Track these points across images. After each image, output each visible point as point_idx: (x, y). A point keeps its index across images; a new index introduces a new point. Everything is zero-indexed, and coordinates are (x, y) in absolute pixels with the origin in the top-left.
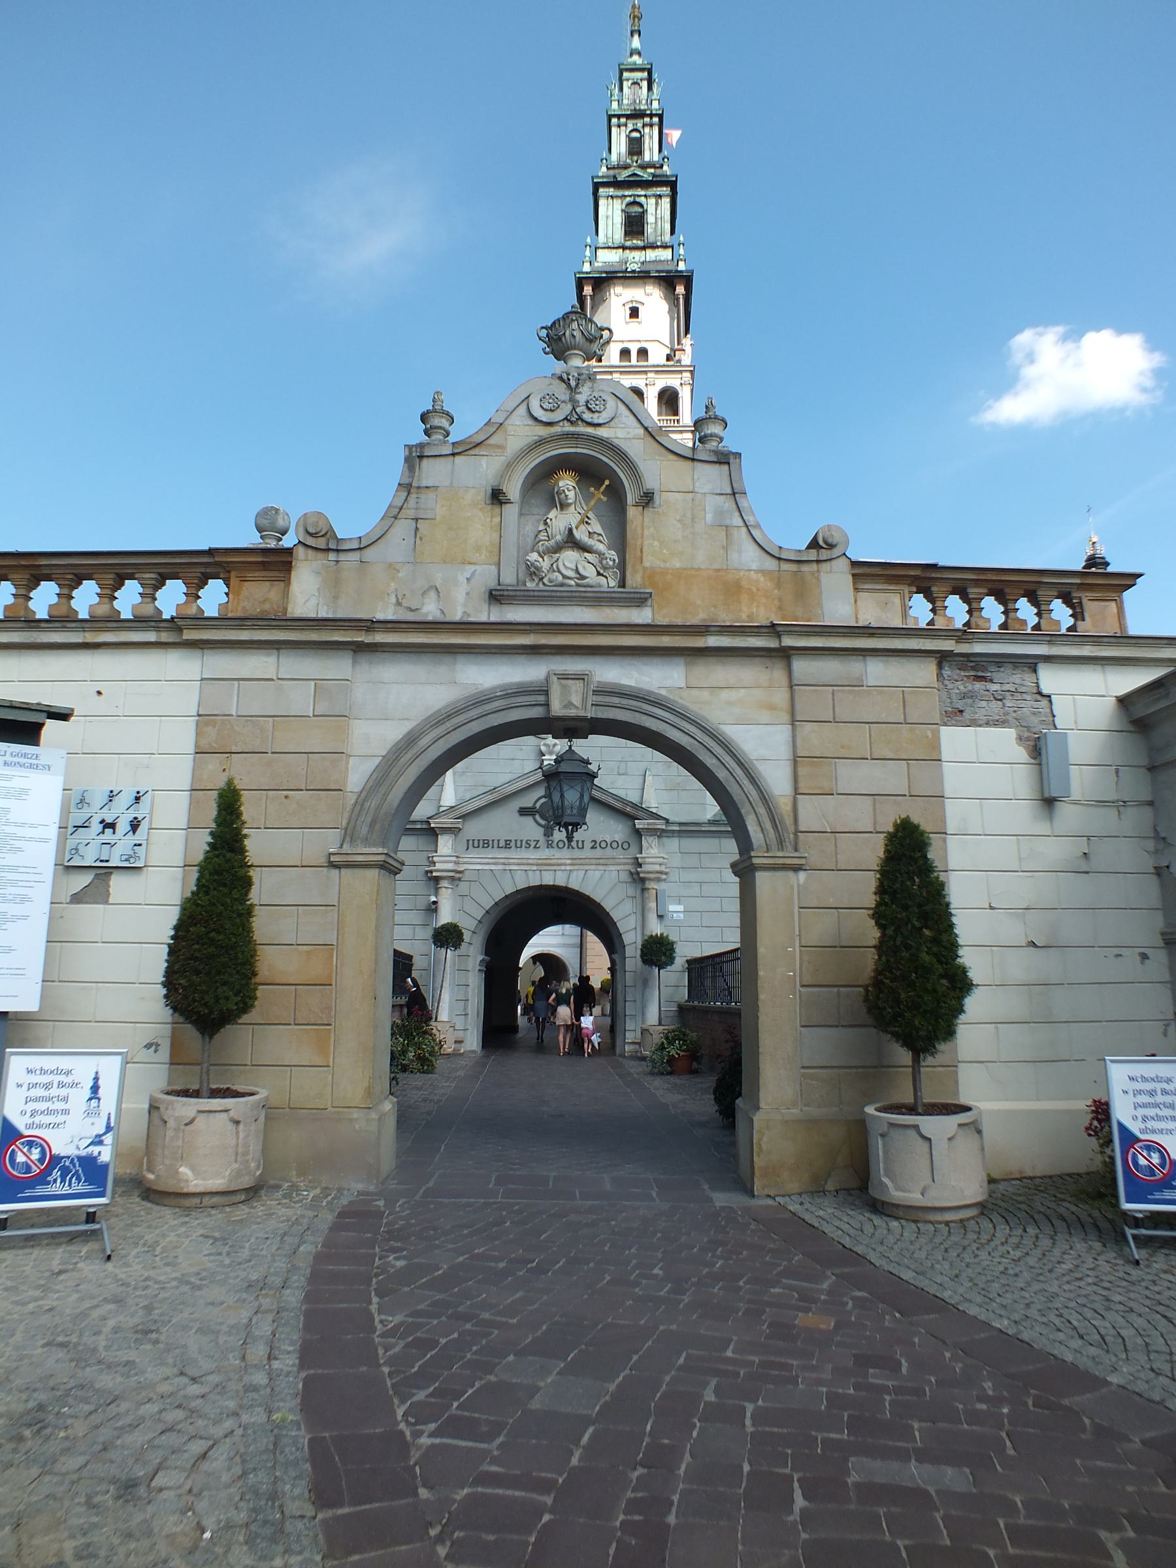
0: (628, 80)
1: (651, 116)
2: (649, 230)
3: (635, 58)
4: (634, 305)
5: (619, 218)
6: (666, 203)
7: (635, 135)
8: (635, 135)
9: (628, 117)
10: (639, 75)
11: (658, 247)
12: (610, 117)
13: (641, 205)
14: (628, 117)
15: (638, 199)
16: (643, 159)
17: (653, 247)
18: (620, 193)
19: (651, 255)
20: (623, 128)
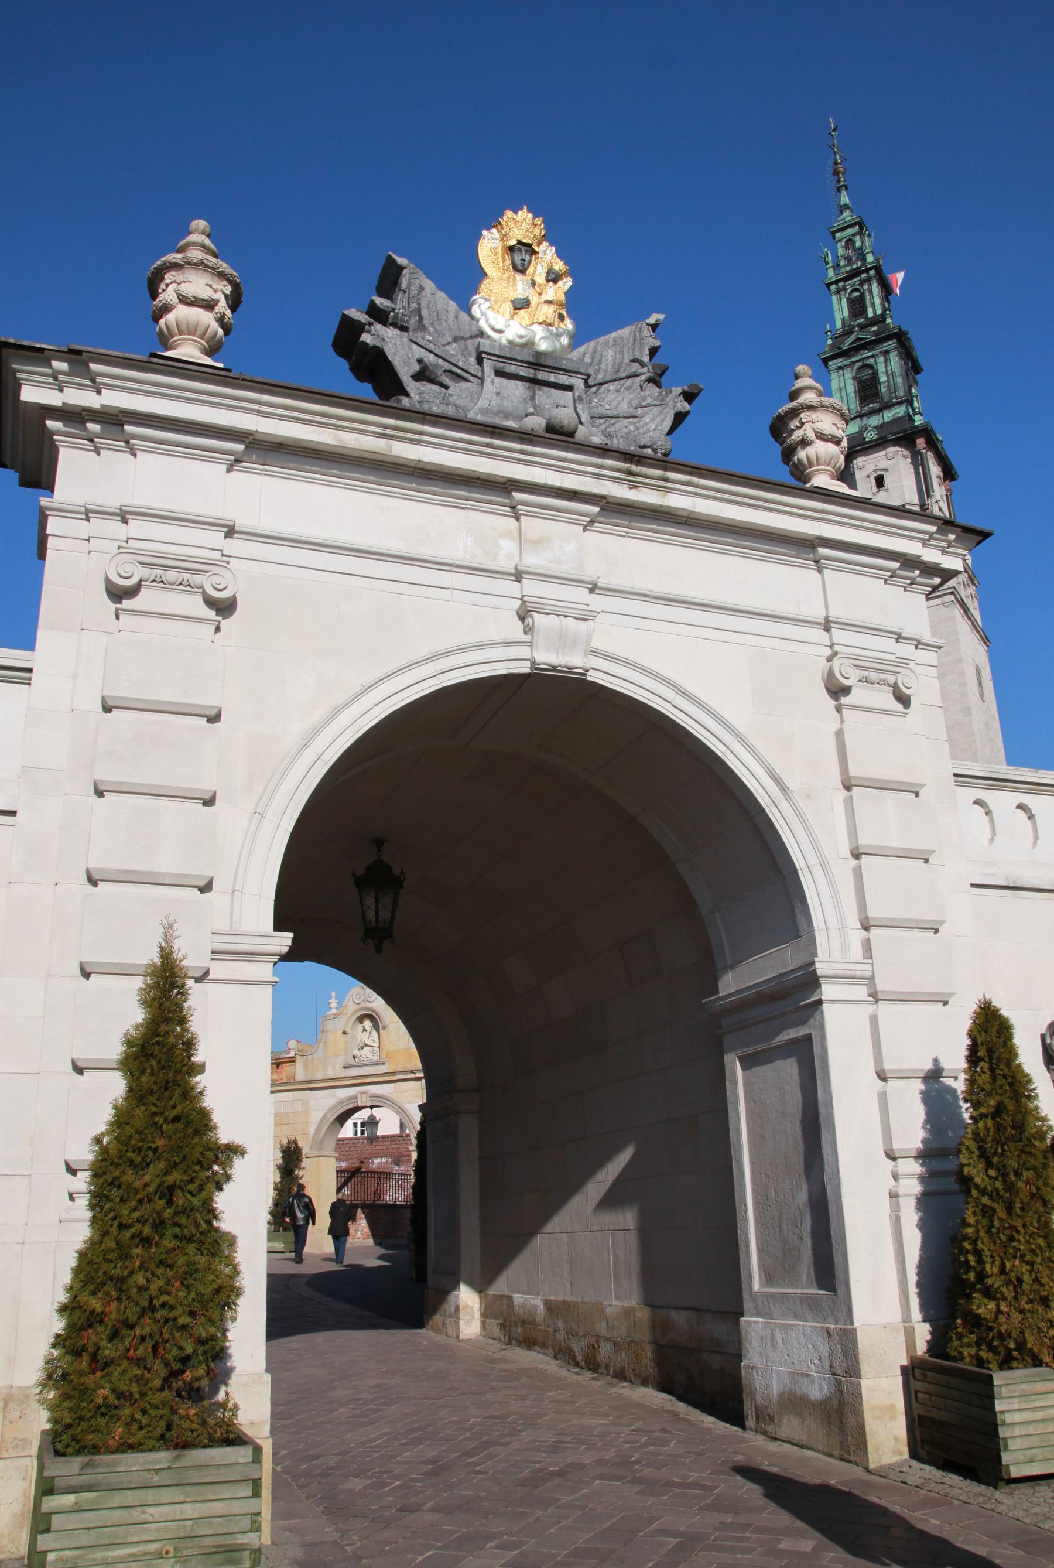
0: (840, 240)
1: (867, 271)
2: (883, 389)
3: (846, 213)
4: (879, 473)
5: (851, 387)
6: (894, 358)
7: (856, 294)
8: (856, 294)
9: (845, 280)
10: (850, 231)
11: (893, 405)
12: (828, 285)
13: (870, 366)
14: (845, 280)
15: (867, 362)
16: (866, 317)
17: (889, 406)
18: (848, 362)
19: (888, 415)
20: (842, 293)
